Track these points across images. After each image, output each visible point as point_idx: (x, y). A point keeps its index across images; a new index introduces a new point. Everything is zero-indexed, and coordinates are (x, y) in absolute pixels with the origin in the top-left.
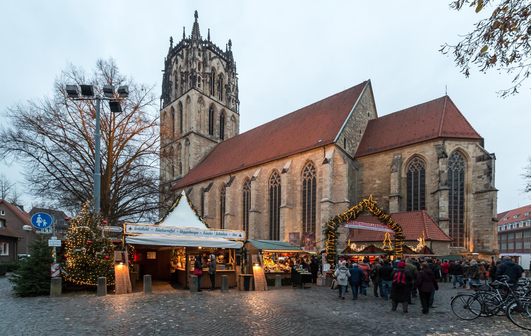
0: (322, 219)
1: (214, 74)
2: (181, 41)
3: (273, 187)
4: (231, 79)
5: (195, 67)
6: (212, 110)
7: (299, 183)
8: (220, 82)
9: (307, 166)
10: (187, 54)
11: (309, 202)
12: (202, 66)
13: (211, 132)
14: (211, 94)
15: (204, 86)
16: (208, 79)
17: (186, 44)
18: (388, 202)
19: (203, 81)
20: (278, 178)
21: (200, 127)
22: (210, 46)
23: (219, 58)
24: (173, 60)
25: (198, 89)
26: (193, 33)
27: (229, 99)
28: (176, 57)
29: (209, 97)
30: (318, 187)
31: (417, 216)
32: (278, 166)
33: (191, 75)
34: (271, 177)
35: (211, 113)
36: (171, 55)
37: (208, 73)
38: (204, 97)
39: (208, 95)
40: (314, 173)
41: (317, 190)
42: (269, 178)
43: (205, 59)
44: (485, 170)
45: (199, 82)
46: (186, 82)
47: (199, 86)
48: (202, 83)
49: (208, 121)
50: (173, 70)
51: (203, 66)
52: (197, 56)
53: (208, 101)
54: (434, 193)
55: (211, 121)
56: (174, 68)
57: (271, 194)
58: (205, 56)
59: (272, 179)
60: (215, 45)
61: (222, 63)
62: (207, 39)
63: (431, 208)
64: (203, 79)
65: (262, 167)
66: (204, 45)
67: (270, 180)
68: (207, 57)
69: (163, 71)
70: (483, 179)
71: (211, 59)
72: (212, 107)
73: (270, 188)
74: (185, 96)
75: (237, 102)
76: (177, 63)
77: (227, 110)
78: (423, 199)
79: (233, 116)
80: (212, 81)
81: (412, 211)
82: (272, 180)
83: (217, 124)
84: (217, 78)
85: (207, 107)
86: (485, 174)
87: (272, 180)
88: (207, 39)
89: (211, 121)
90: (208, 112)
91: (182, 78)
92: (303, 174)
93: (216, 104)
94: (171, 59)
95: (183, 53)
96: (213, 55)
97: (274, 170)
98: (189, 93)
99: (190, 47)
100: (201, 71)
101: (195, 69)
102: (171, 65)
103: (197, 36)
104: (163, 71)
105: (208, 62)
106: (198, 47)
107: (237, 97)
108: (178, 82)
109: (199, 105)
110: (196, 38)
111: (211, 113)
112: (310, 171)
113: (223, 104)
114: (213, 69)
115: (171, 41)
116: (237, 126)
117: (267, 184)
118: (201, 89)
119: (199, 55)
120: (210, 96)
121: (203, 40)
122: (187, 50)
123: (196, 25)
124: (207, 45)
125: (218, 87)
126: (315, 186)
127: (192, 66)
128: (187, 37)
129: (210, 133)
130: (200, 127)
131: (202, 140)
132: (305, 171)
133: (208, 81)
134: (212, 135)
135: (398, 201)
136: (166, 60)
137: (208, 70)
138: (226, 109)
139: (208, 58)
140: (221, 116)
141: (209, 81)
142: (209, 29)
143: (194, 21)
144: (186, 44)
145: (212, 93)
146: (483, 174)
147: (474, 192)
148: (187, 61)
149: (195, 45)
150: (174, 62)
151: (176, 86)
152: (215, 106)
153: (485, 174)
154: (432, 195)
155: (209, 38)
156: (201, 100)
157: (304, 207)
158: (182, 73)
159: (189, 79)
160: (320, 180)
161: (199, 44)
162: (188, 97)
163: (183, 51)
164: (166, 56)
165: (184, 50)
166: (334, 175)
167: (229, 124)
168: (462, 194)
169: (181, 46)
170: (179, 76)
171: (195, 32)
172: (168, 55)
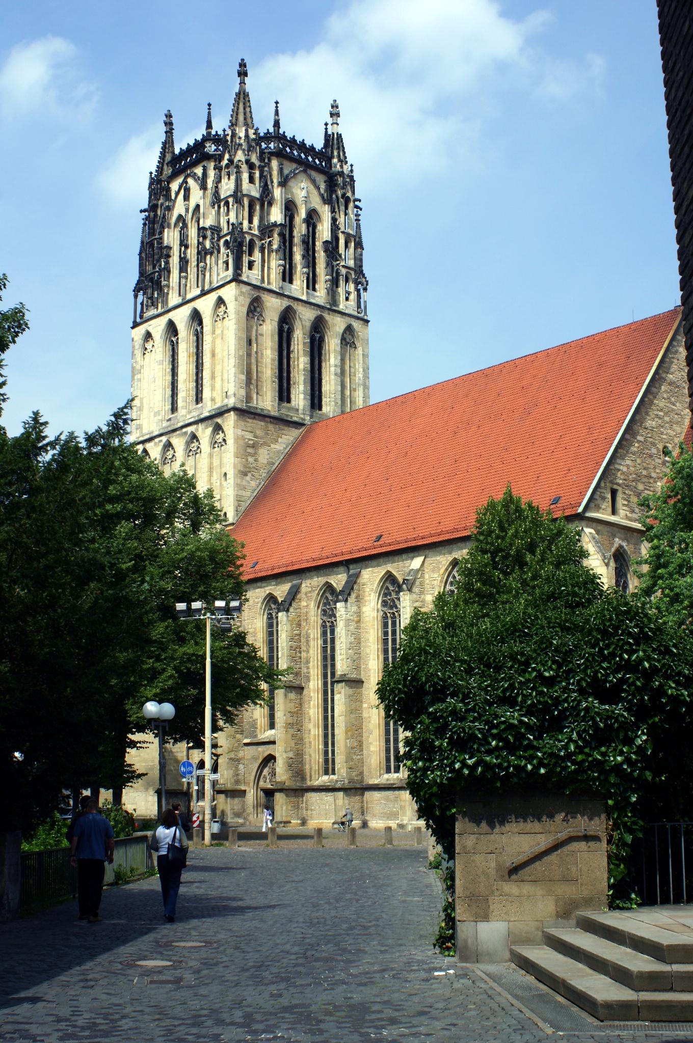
1: (292, 218)
6: (286, 327)
10: (218, 180)
23: (305, 171)
33: (228, 238)
35: (285, 334)
37: (275, 225)
43: (266, 185)
51: (262, 206)
55: (285, 361)
60: (293, 140)
61: (314, 182)
62: (271, 130)
71: (283, 183)
74: (212, 298)
80: (285, 245)
84: (300, 229)
88: (271, 130)
89: (285, 361)
96: (289, 167)
98: (222, 292)
105: (277, 193)
111: (285, 334)
114: (290, 208)
122: (218, 168)
125: (304, 257)
133: (275, 247)
137: (276, 215)
142: (277, 103)
145: (288, 275)
155: (277, 124)
159: (222, 249)
162: (220, 301)
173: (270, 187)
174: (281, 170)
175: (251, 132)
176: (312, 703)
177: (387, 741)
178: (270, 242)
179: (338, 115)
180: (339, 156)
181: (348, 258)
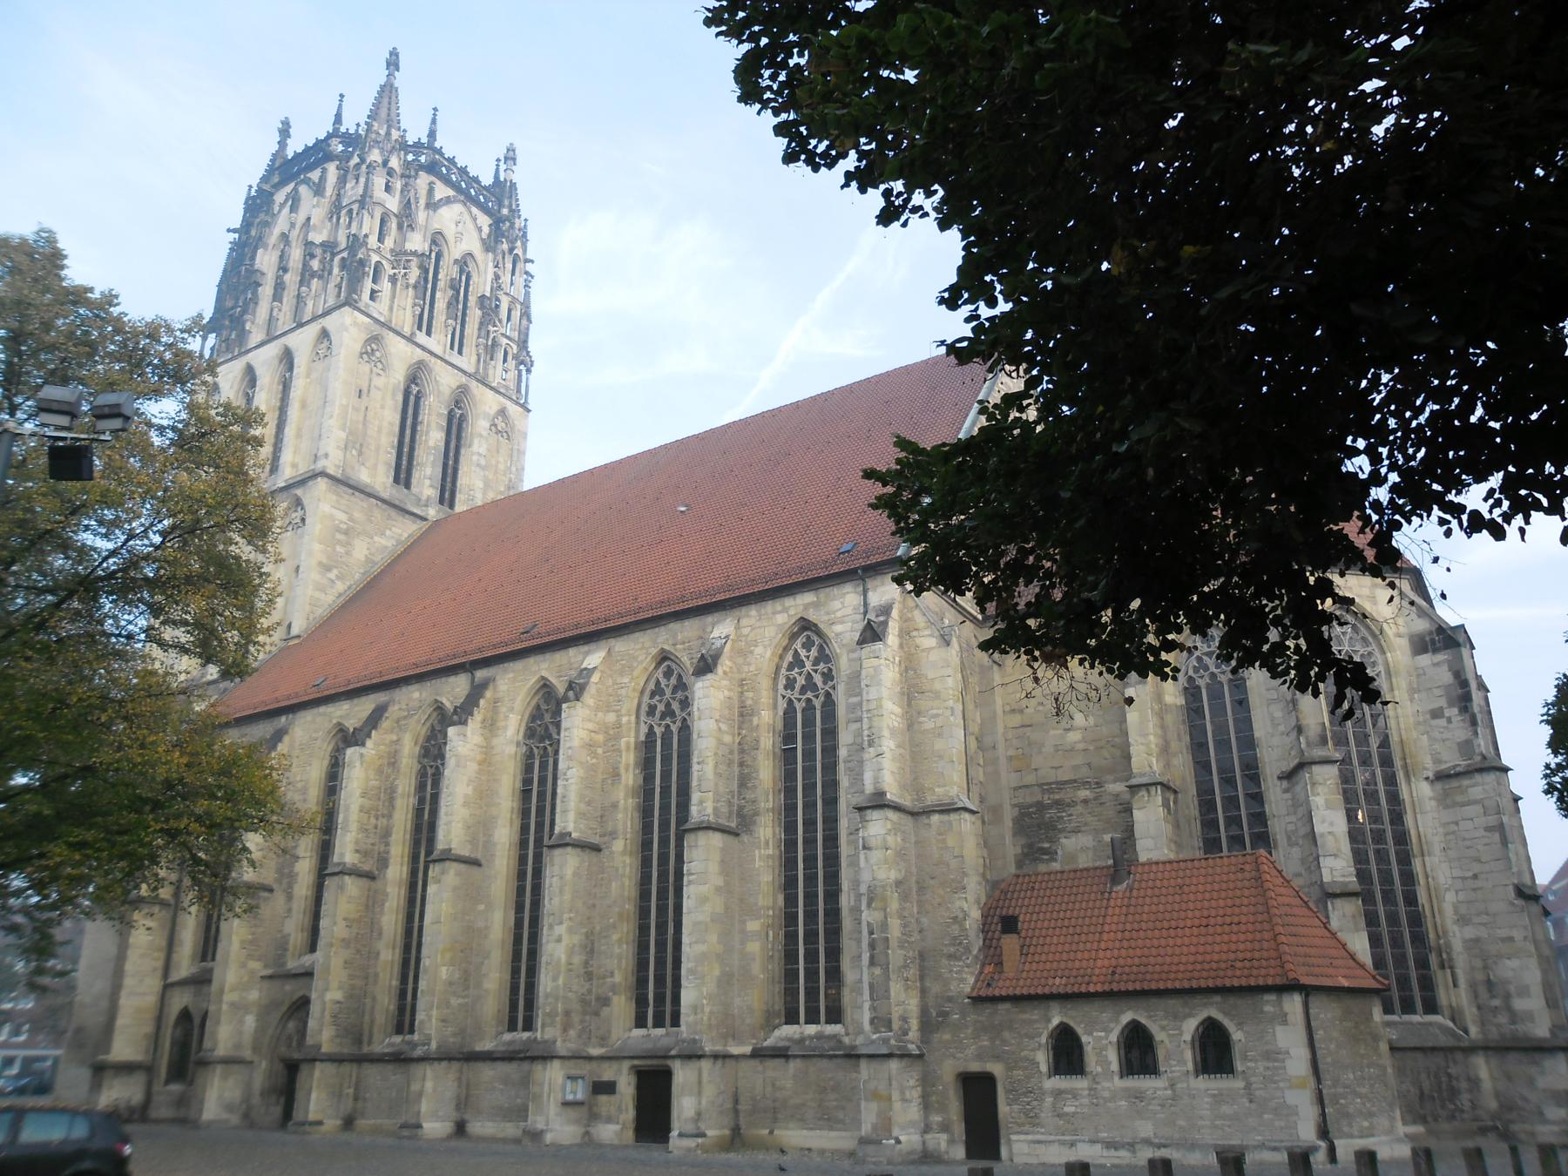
0: (863, 889)
2: (322, 137)
3: (658, 731)
4: (506, 278)
5: (365, 230)
6: (415, 389)
7: (767, 718)
8: (459, 288)
9: (798, 645)
10: (342, 181)
11: (810, 806)
12: (394, 226)
13: (403, 474)
14: (420, 328)
15: (393, 296)
16: (414, 274)
17: (340, 148)
18: (1128, 810)
19: (393, 279)
20: (679, 695)
21: (360, 453)
22: (433, 162)
24: (280, 197)
25: (367, 306)
26: (373, 116)
27: (491, 349)
28: (295, 190)
29: (410, 339)
30: (845, 737)
31: (1240, 875)
32: (682, 638)
34: (652, 686)
36: (276, 179)
37: (414, 253)
38: (391, 337)
39: (407, 330)
40: (828, 676)
41: (842, 752)
42: (642, 692)
44: (1447, 687)
45: (374, 281)
46: (320, 277)
47: (373, 295)
48: (386, 285)
49: (397, 429)
50: (276, 232)
51: (400, 227)
52: (379, 192)
53: (401, 354)
54: (1290, 776)
56: (281, 225)
57: (646, 764)
58: (412, 194)
59: (653, 694)
62: (424, 140)
63: (1289, 838)
64: (392, 272)
65: (612, 642)
66: (410, 157)
67: (646, 699)
68: (417, 200)
69: (234, 231)
70: (1449, 720)
72: (416, 376)
73: (642, 738)
75: (522, 363)
76: (294, 209)
77: (477, 389)
78: (1257, 798)
79: (502, 412)
81: (1225, 852)
82: (654, 701)
83: (431, 443)
85: (399, 375)
86: (1451, 705)
87: (654, 701)
88: (424, 140)
90: (400, 398)
91: (305, 265)
92: (782, 682)
93: (437, 365)
94: (272, 194)
95: (323, 178)
96: (442, 191)
97: (665, 659)
99: (356, 160)
100: (389, 243)
101: (366, 236)
102: (269, 211)
103: (389, 127)
104: (234, 231)
105: (421, 216)
106: (385, 163)
107: (523, 344)
108: (287, 277)
109: (367, 368)
110: (382, 132)
112: (808, 666)
113: (464, 366)
115: (285, 131)
116: (517, 455)
117: (633, 718)
118: (380, 309)
119: (388, 188)
120: (413, 334)
121: (411, 139)
123: (387, 92)
124: (423, 159)
126: (831, 733)
127: (354, 224)
128: (348, 125)
129: (396, 480)
130: (360, 453)
131: (360, 504)
132: (790, 667)
133: (412, 281)
134: (408, 485)
135: (1166, 804)
136: (253, 193)
137: (417, 242)
138: (473, 384)
139: (422, 202)
140: (451, 412)
141: (418, 282)
143: (383, 80)
144: (340, 148)
146: (1443, 702)
147: (1431, 775)
148: (336, 208)
149: (375, 156)
150: (282, 205)
151: (279, 287)
152: (430, 371)
153: (1451, 705)
154: (1285, 784)
155: (432, 134)
156: (372, 347)
157: (790, 828)
158: (308, 244)
160: (853, 708)
161: (391, 152)
163: (324, 171)
164: (255, 182)
165: (332, 168)
166: (912, 691)
167: (478, 446)
168: (1391, 780)
169: (318, 154)
170: (296, 254)
171: (383, 113)
172: (264, 179)
173: (413, 207)
174: (431, 191)
175: (395, 134)
176: (387, 904)
177: (515, 972)
178: (405, 274)
179: (514, 159)
180: (510, 205)
181: (505, 330)
